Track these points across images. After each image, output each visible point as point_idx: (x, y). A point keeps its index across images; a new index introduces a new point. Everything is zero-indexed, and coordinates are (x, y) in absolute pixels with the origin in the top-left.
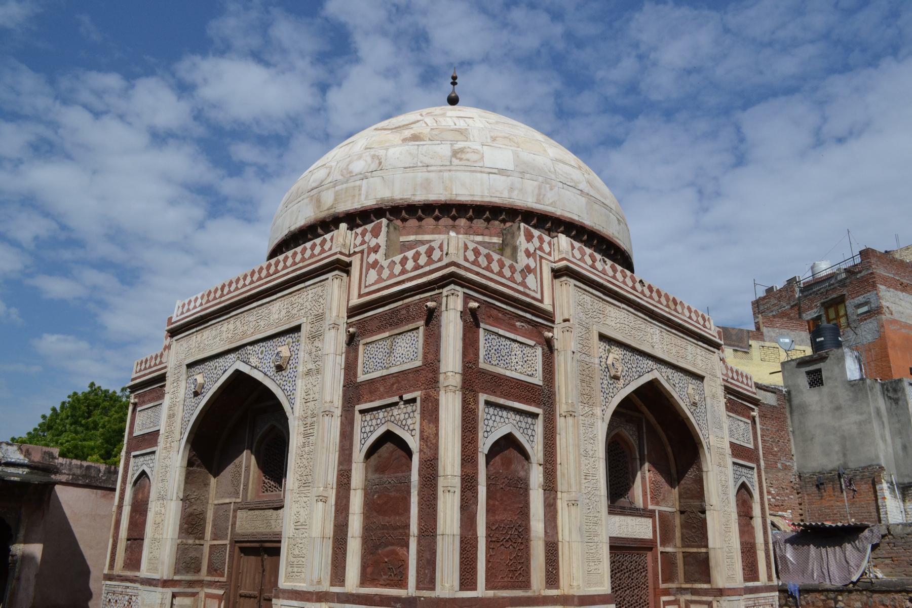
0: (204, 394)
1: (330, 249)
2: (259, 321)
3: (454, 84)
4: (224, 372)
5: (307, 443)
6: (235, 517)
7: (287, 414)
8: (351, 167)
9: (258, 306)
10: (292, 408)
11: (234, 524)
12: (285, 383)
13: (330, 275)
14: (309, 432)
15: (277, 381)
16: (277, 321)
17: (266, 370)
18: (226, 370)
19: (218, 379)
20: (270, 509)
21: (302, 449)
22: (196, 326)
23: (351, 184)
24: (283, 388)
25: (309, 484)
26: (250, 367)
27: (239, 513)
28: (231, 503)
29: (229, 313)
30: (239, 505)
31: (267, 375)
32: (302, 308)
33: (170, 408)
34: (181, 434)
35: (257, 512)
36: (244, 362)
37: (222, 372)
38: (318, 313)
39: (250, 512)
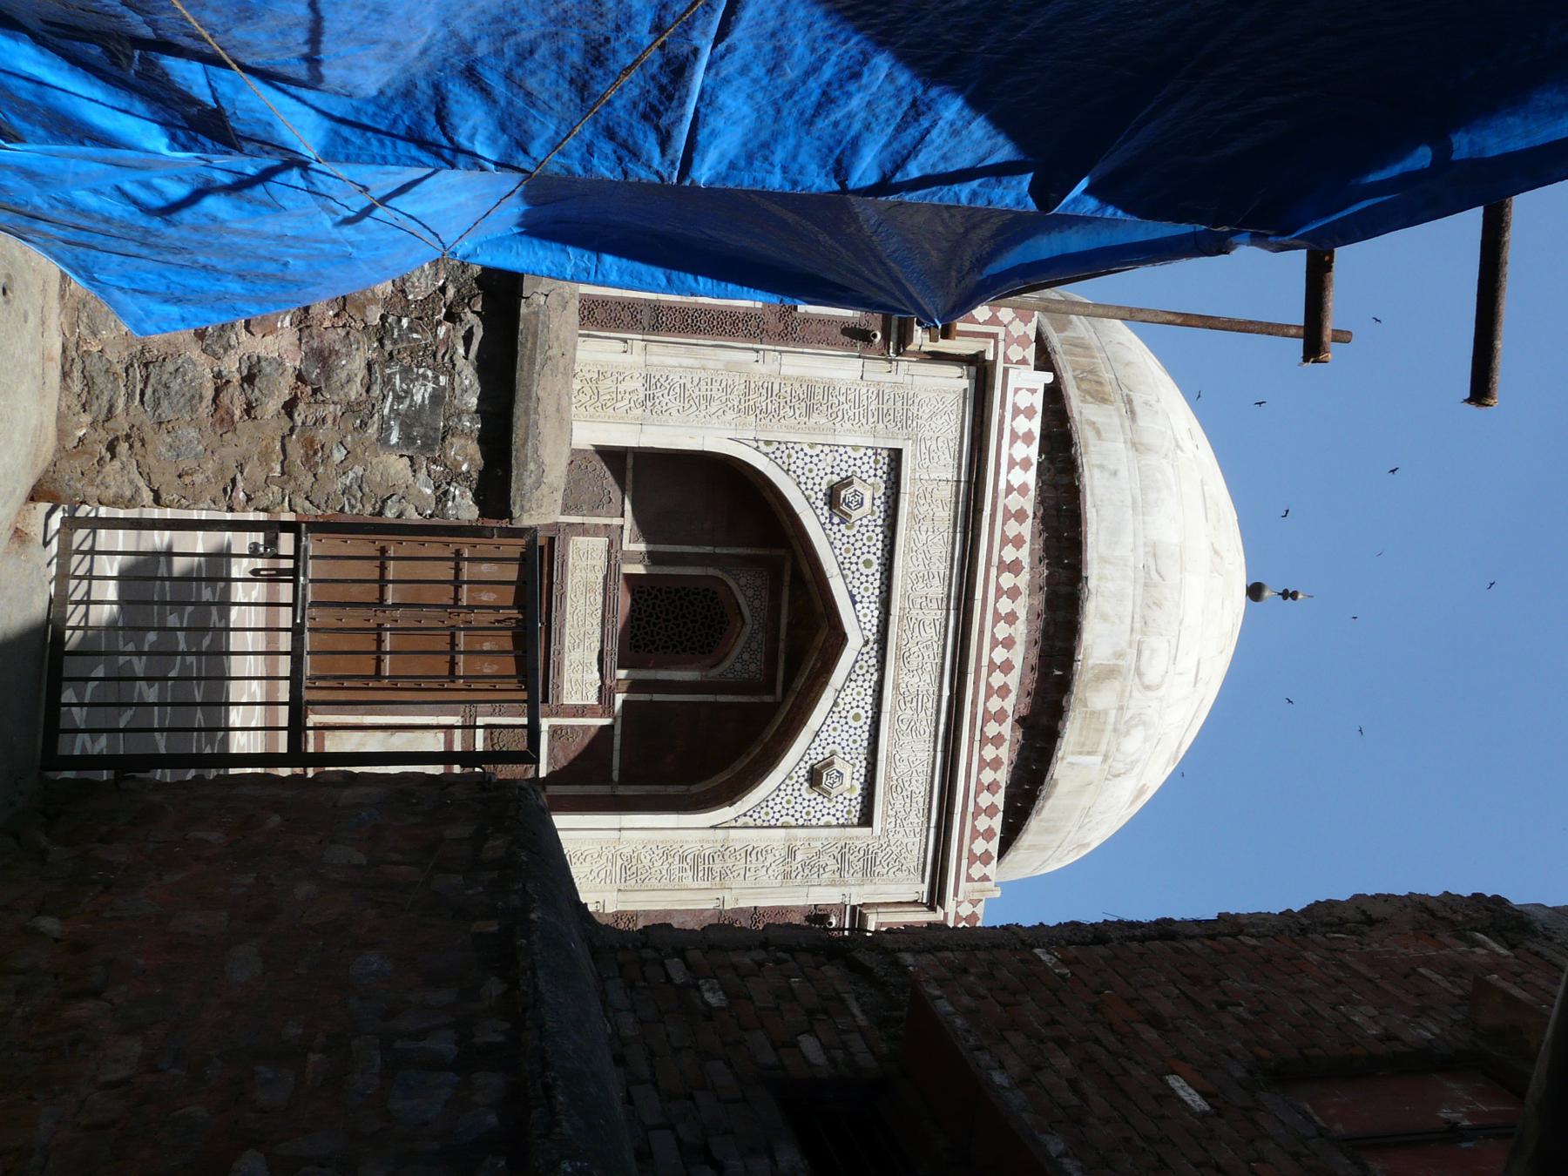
0: (828, 526)
1: (969, 879)
2: (914, 704)
3: (1285, 595)
4: (852, 597)
5: (685, 865)
6: (594, 531)
7: (739, 803)
8: (1138, 734)
9: (940, 696)
10: (745, 815)
11: (584, 530)
12: (789, 791)
13: (925, 888)
14: (701, 868)
15: (797, 769)
16: (897, 756)
17: (823, 736)
18: (854, 603)
19: (844, 577)
20: (602, 642)
21: (677, 858)
22: (969, 482)
23: (1110, 727)
24: (783, 787)
25: (623, 880)
26: (839, 687)
27: (601, 542)
28: (622, 515)
29: (957, 609)
30: (616, 546)
31: (813, 741)
32: (899, 821)
33: (829, 389)
34: (768, 443)
35: (600, 599)
36: (857, 661)
37: (855, 591)
38: (878, 863)
39: (601, 580)
